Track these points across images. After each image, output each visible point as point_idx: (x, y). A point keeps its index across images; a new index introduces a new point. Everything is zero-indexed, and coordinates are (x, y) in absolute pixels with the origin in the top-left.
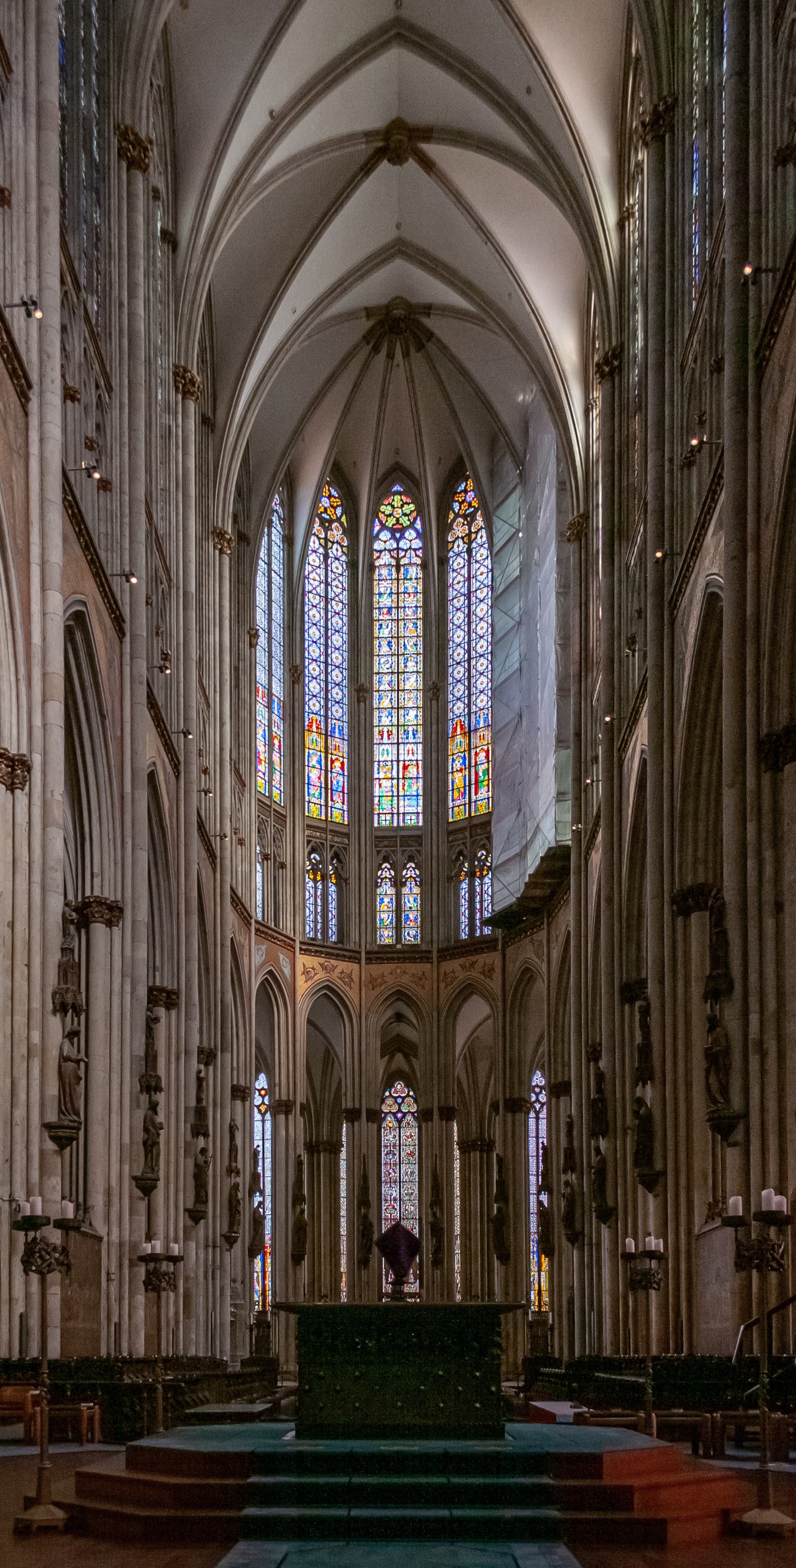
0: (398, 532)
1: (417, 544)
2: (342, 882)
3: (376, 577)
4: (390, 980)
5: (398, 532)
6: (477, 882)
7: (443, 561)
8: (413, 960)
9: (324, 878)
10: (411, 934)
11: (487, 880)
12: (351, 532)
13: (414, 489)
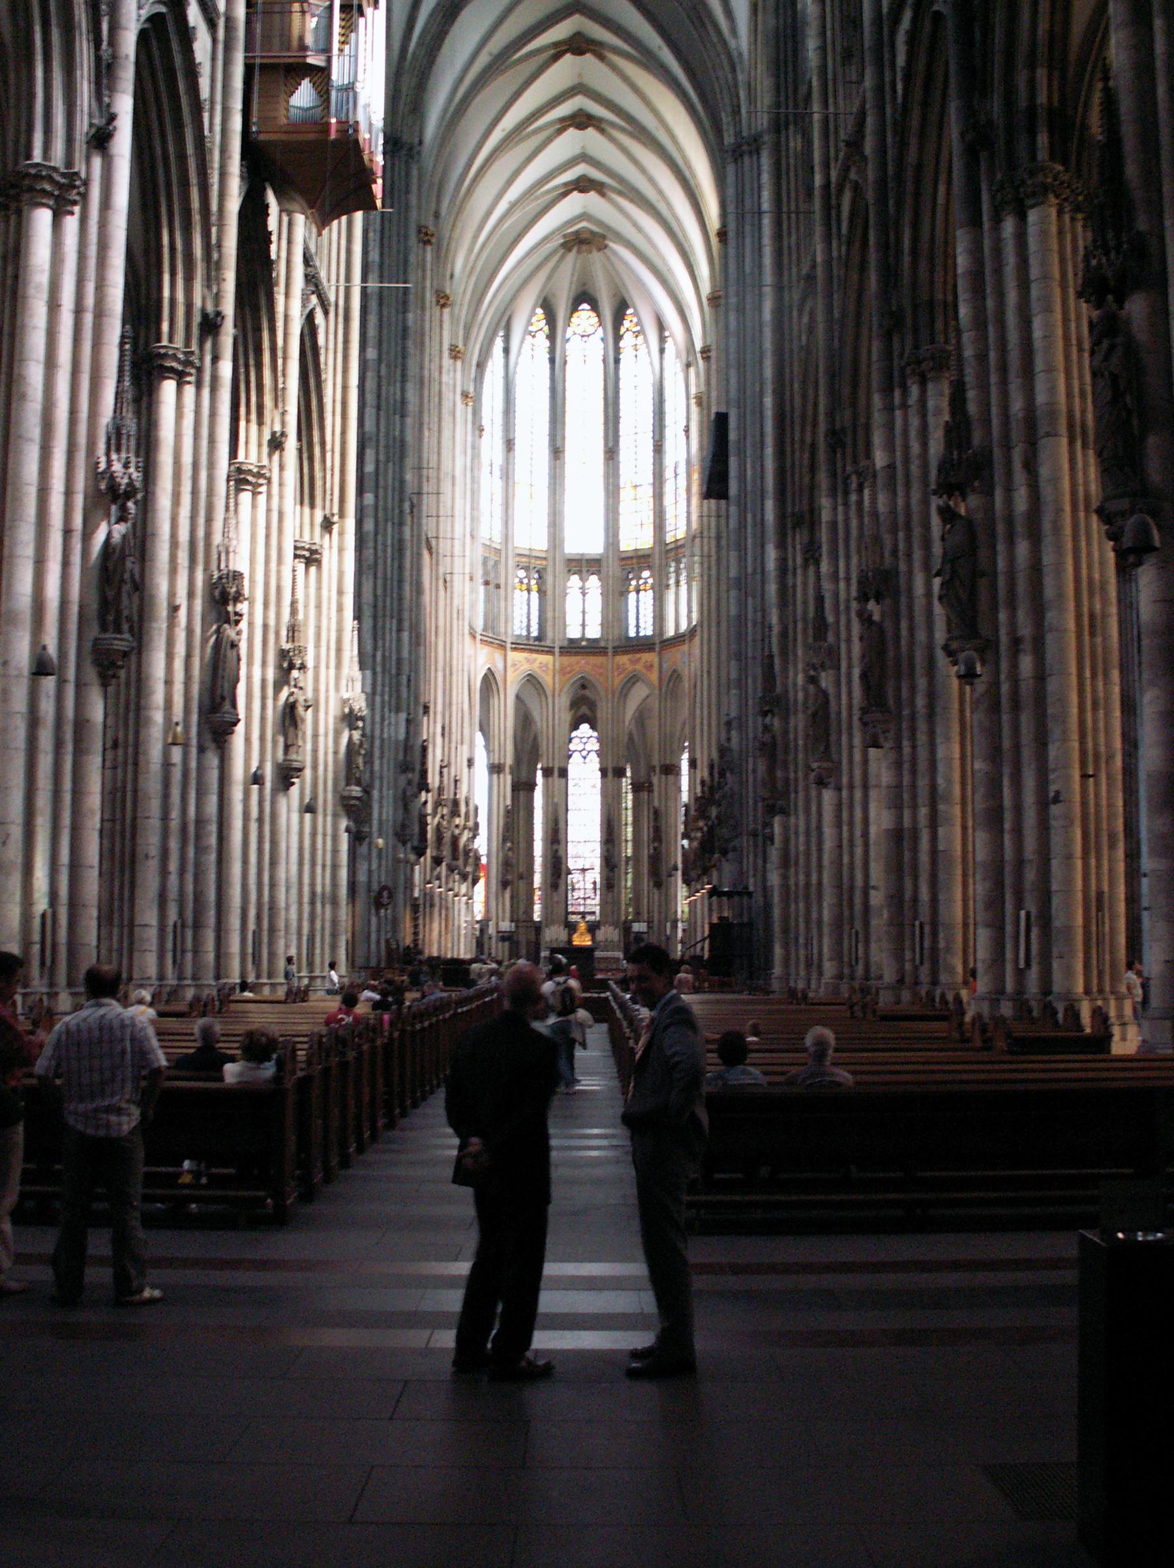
2: (542, 592)
4: (577, 668)
7: (617, 361)
8: (594, 654)
9: (529, 590)
12: (552, 337)
13: (595, 308)
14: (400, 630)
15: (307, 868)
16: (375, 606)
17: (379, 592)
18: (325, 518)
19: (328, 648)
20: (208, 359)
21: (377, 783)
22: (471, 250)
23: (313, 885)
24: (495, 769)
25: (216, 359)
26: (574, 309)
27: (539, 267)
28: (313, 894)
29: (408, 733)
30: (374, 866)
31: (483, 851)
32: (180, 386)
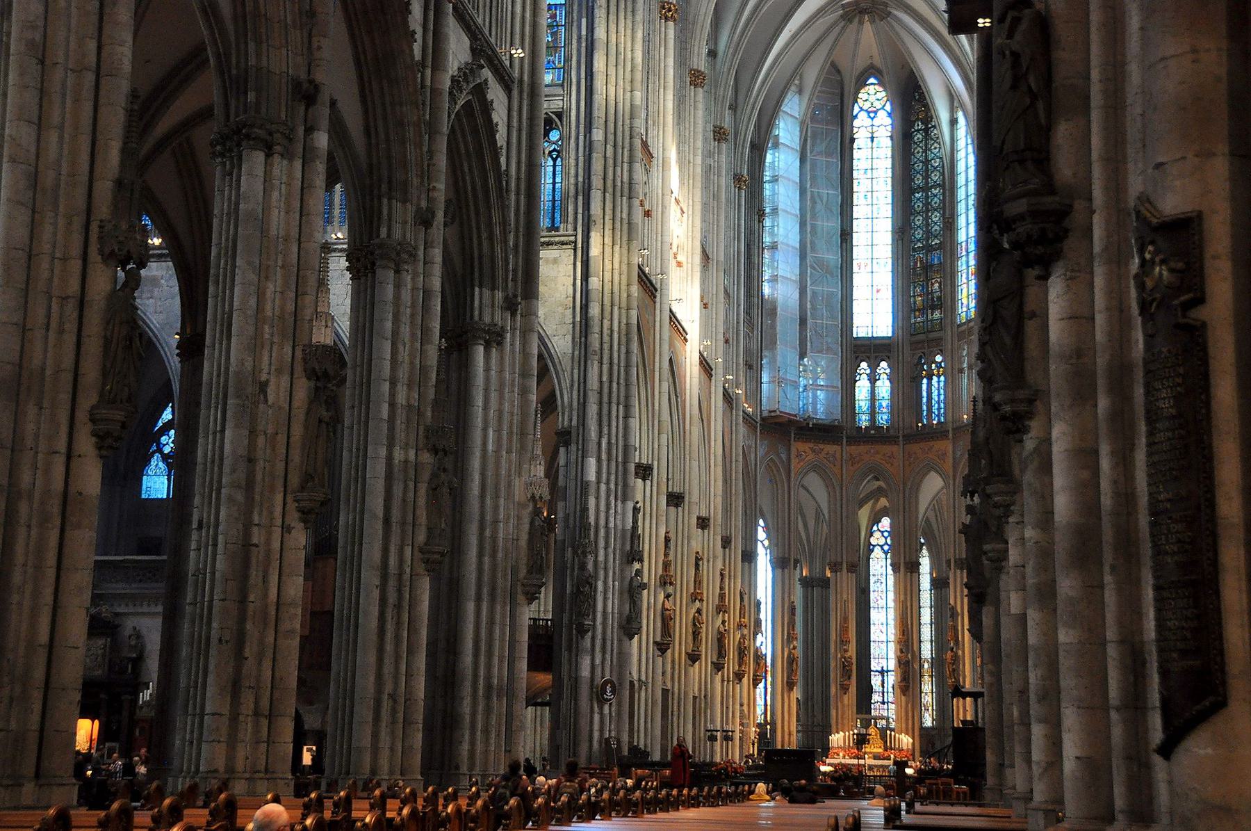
0: (873, 114)
1: (889, 121)
3: (855, 146)
5: (873, 114)
6: (935, 379)
10: (883, 419)
11: (942, 378)
14: (627, 416)
15: (482, 658)
16: (600, 393)
17: (605, 378)
18: (506, 298)
19: (511, 433)
20: (301, 131)
21: (602, 573)
22: (734, 27)
23: (488, 678)
24: (782, 563)
25: (309, 130)
26: (861, 83)
27: (819, 41)
28: (489, 687)
29: (635, 522)
30: (598, 661)
31: (767, 650)
32: (268, 155)
